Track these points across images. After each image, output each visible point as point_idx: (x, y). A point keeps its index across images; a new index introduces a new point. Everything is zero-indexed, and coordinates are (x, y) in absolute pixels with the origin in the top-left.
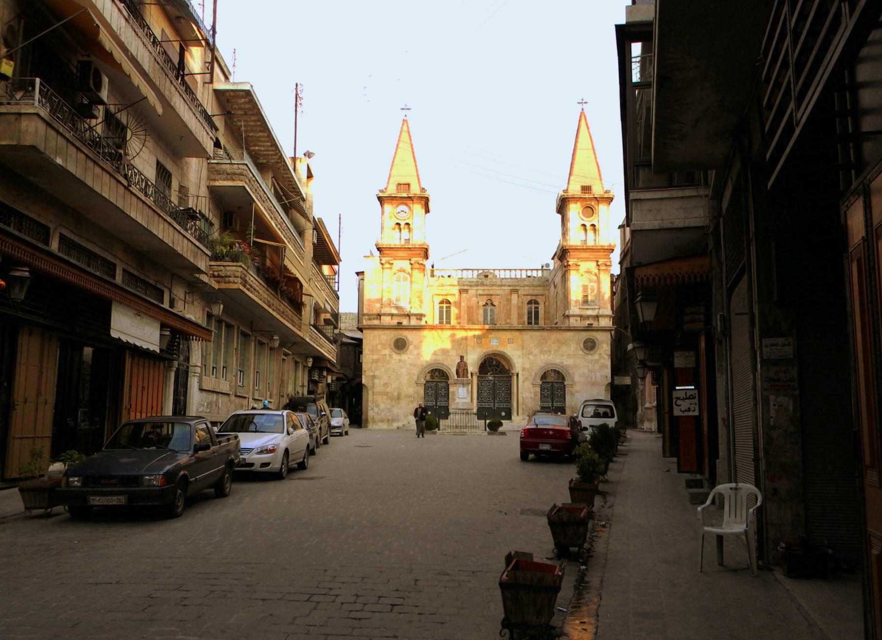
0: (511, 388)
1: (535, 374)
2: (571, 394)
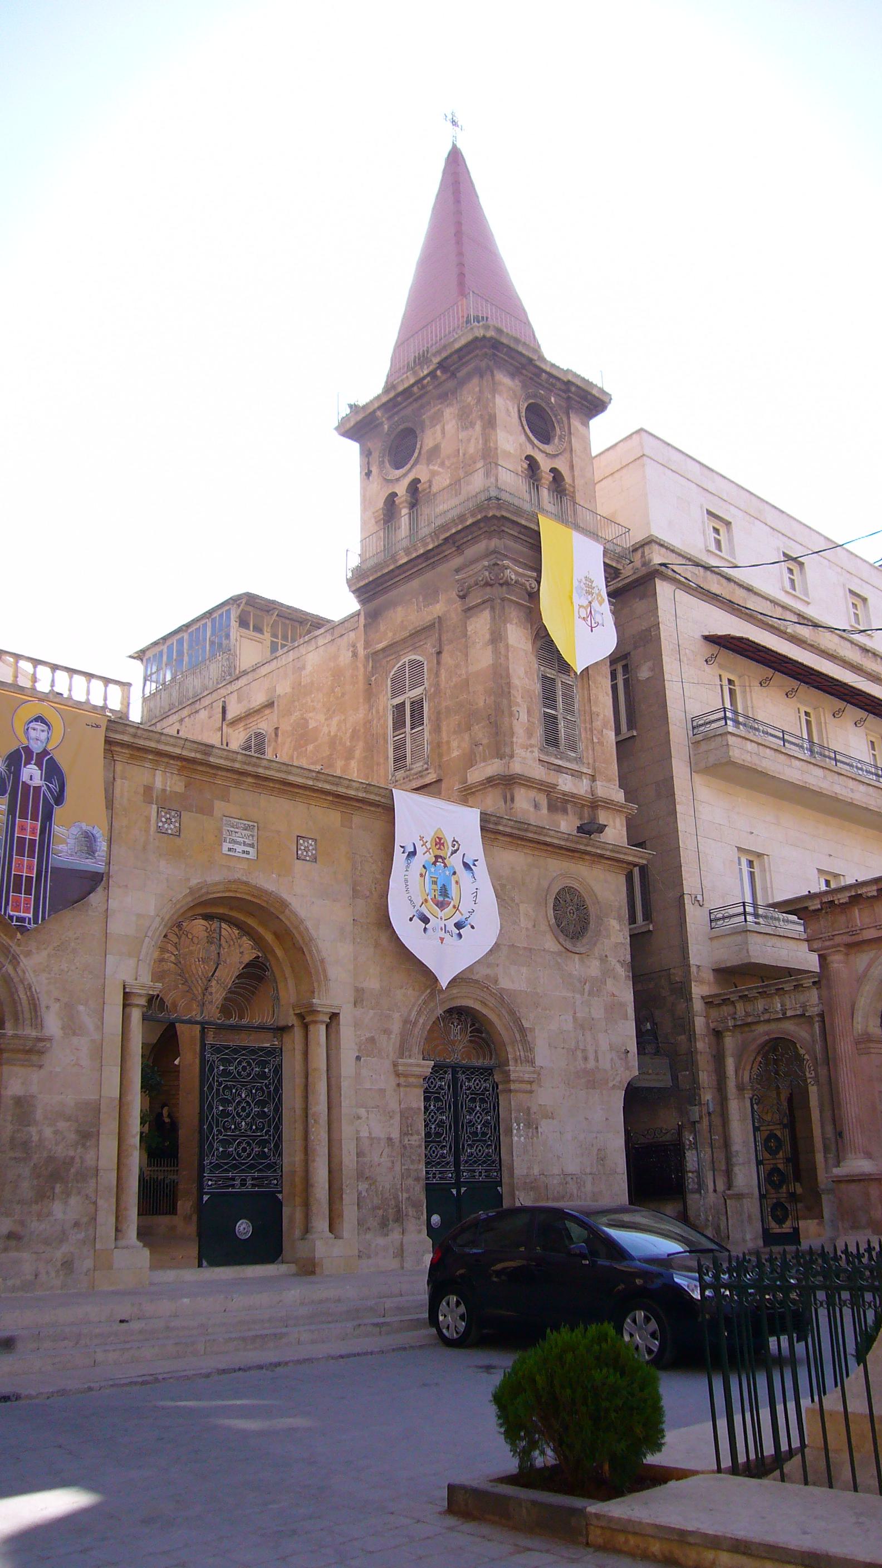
0: (278, 1088)
1: (406, 1022)
2: (528, 1125)
